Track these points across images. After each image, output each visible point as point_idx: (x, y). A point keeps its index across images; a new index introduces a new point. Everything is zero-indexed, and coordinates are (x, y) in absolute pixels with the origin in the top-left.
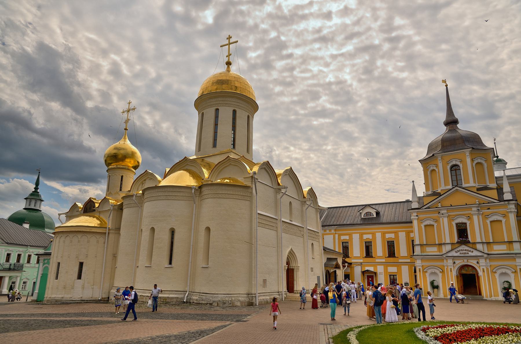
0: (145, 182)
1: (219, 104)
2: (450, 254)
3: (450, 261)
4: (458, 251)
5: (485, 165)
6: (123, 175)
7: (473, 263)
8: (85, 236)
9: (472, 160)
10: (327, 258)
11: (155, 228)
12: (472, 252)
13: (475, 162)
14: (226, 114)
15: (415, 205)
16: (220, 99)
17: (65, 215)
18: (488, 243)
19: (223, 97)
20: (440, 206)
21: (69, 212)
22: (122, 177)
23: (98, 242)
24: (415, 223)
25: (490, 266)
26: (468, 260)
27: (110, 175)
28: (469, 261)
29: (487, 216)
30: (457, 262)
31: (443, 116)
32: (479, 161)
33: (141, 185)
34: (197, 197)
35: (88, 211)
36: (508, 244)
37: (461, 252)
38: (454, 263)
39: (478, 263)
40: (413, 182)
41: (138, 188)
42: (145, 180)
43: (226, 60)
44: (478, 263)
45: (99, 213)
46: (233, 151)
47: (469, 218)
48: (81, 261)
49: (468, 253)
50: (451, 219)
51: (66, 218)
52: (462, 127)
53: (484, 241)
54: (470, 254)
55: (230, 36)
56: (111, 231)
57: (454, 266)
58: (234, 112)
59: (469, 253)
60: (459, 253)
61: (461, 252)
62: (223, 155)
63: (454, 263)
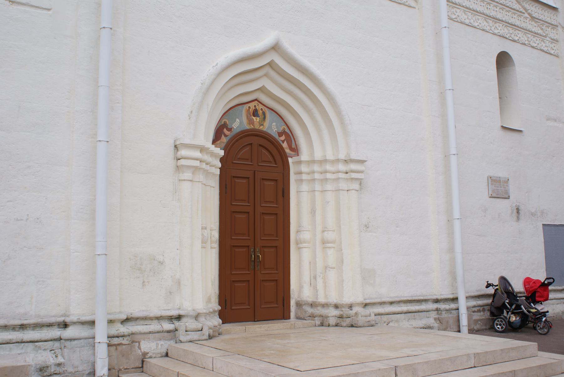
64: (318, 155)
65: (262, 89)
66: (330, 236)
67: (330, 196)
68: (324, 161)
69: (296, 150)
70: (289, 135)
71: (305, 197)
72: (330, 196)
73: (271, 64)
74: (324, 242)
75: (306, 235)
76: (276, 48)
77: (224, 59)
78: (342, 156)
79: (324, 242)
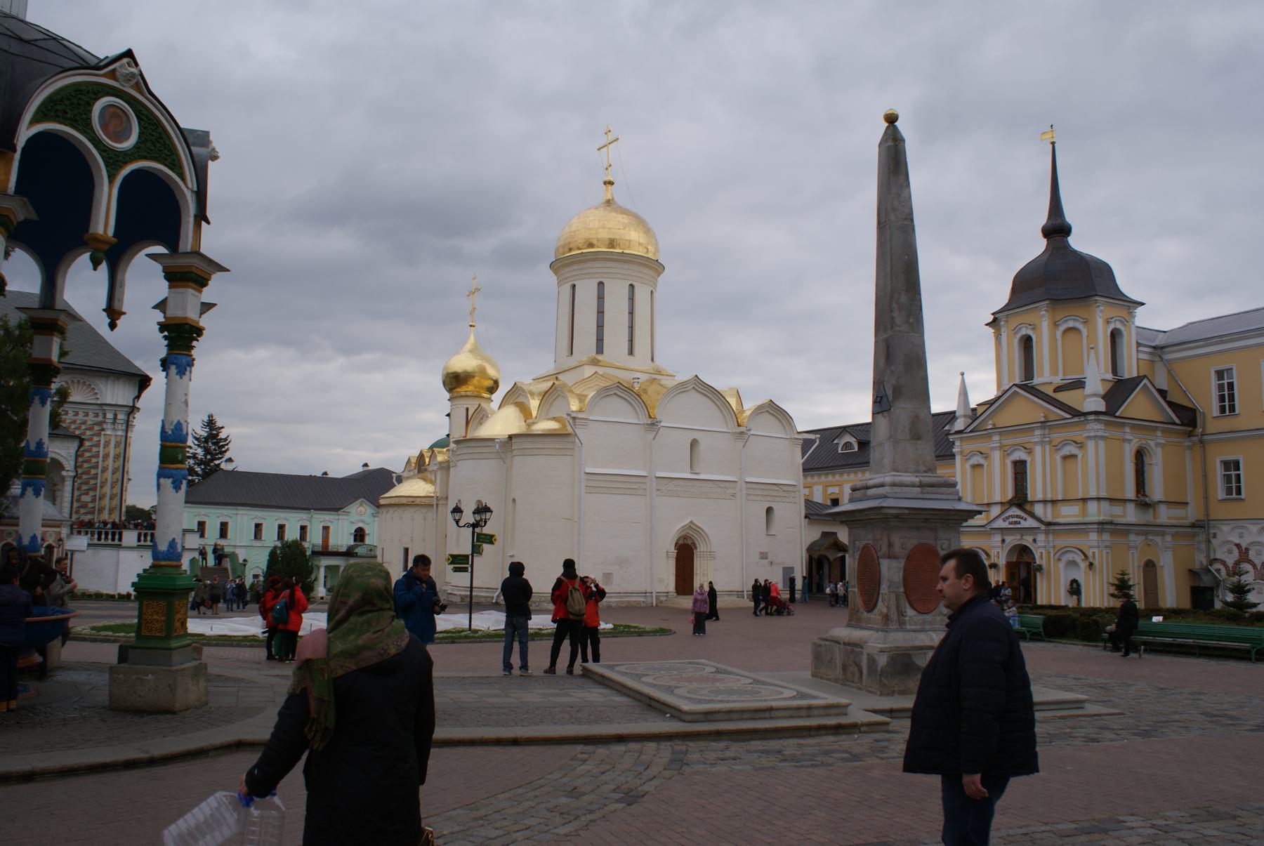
2: (996, 525)
3: (997, 538)
4: (1006, 518)
5: (1085, 331)
7: (1027, 541)
9: (1055, 324)
10: (823, 532)
12: (1025, 520)
13: (1062, 328)
14: (587, 291)
15: (959, 425)
16: (575, 267)
18: (1054, 502)
19: (580, 262)
20: (990, 427)
24: (958, 458)
25: (1054, 547)
26: (1022, 536)
28: (1024, 537)
29: (1057, 448)
30: (1008, 539)
31: (1042, 219)
32: (1071, 324)
36: (1081, 503)
37: (1011, 520)
38: (1003, 541)
39: (1035, 541)
40: (962, 374)
44: (1035, 541)
46: (600, 357)
47: (1030, 452)
48: (406, 546)
49: (1020, 523)
50: (1006, 453)
52: (1077, 242)
53: (1049, 497)
54: (1024, 524)
56: (440, 502)
57: (1002, 547)
58: (601, 284)
59: (1022, 521)
60: (1008, 521)
61: (1011, 520)
62: (567, 373)
63: (1003, 541)
64: (702, 550)
65: (688, 533)
66: (705, 572)
67: (705, 561)
68: (703, 552)
69: (696, 548)
70: (694, 544)
71: (698, 561)
72: (705, 561)
73: (690, 526)
74: (703, 574)
75: (698, 572)
76: (691, 522)
77: (678, 528)
78: (709, 550)
79: (703, 574)
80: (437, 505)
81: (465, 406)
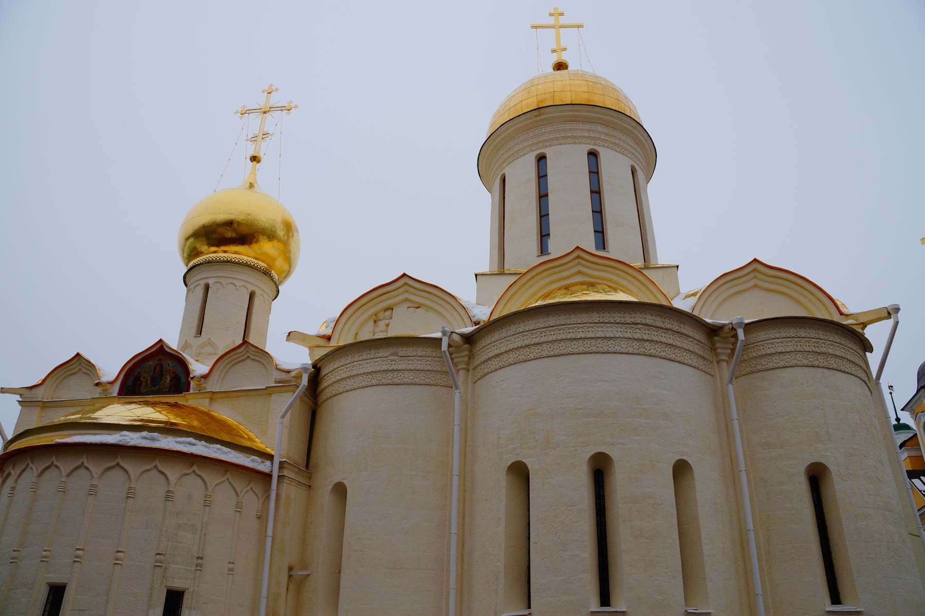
0: (388, 313)
1: (599, 139)
6: (258, 292)
8: (193, 476)
11: (532, 465)
17: (18, 398)
19: (606, 124)
21: (42, 388)
22: (252, 296)
23: (239, 508)
27: (210, 281)
33: (371, 323)
34: (724, 364)
35: (143, 390)
41: (357, 334)
42: (390, 308)
43: (554, 59)
45: (207, 401)
48: (177, 584)
51: (21, 409)
55: (552, 11)
80: (280, 477)
81: (251, 288)
